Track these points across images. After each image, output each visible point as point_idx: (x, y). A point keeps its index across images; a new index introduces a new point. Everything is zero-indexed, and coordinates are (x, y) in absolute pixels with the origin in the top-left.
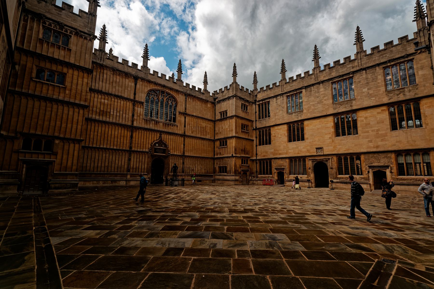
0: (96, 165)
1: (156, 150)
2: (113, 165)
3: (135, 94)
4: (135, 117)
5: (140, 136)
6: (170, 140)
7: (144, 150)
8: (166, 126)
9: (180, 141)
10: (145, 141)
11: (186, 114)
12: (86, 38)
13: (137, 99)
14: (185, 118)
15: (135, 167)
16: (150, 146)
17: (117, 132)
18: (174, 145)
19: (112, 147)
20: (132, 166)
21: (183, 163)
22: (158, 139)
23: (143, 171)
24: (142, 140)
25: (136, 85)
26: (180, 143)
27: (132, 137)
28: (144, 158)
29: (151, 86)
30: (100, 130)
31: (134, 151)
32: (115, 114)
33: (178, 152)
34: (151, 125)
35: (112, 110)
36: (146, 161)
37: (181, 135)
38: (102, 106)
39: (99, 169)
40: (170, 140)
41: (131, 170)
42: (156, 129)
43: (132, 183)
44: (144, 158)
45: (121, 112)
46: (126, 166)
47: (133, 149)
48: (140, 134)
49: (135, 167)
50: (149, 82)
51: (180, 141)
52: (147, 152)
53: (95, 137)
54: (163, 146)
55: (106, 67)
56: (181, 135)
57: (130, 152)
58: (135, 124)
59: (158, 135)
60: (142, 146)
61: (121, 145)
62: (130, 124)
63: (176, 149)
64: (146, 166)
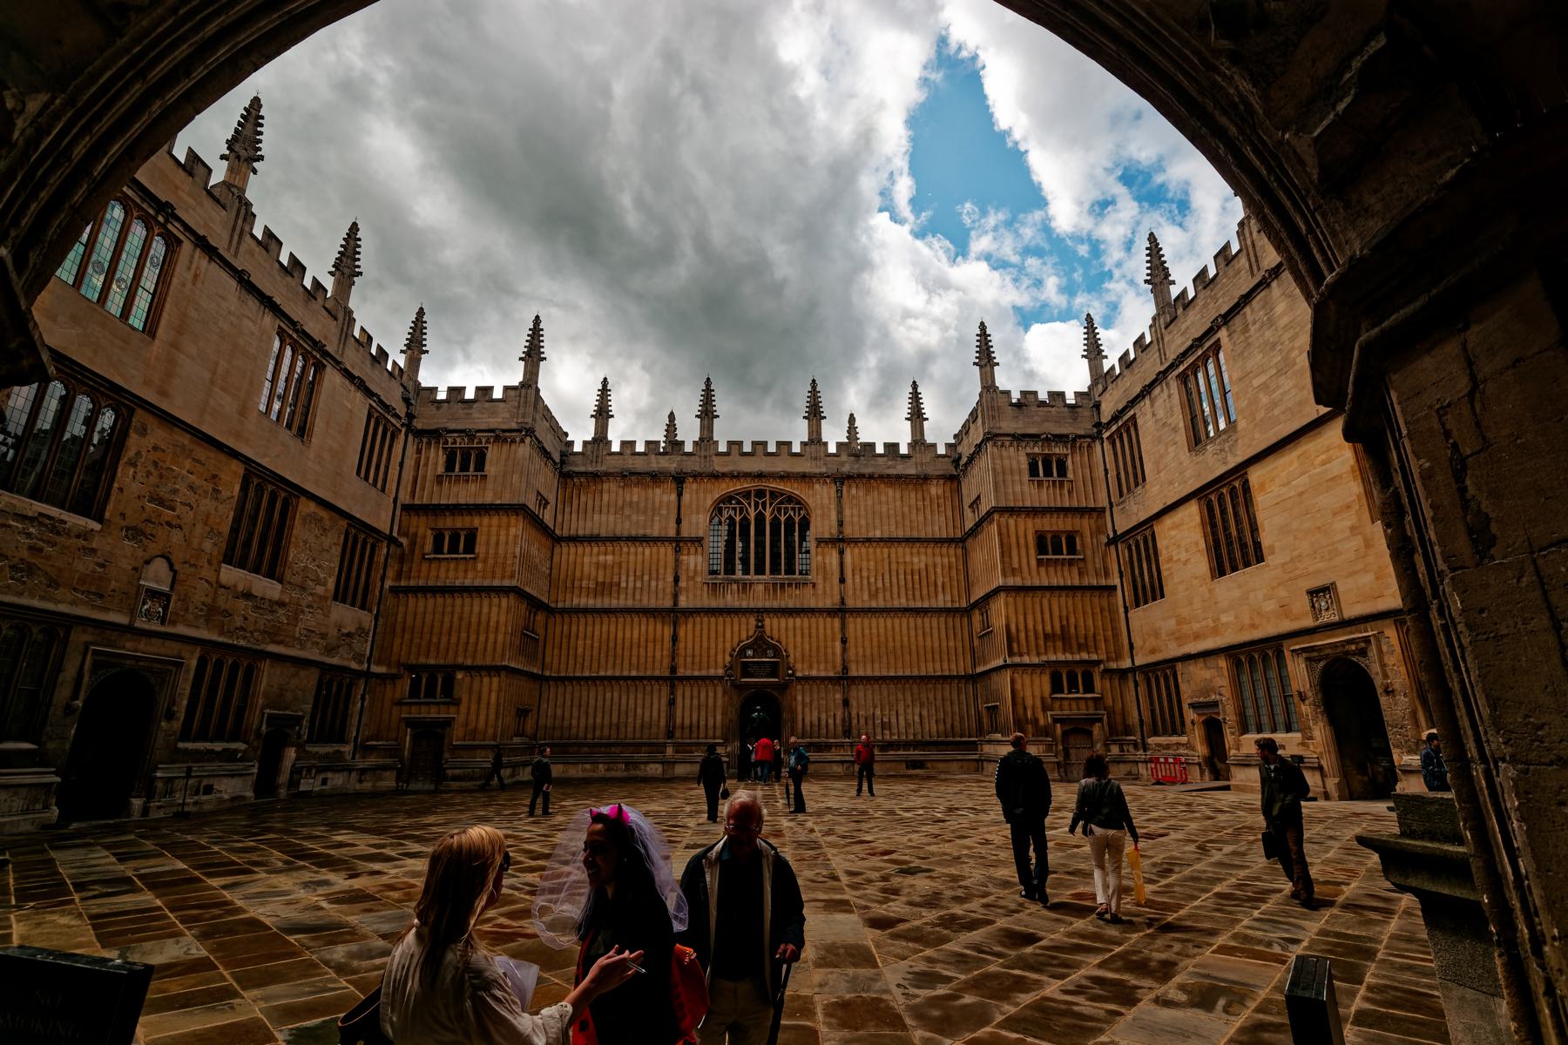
0: (591, 721)
1: (746, 669)
2: (630, 720)
3: (679, 521)
4: (682, 584)
5: (697, 633)
6: (791, 633)
7: (712, 672)
8: (775, 591)
10: (713, 645)
11: (842, 540)
12: (513, 441)
13: (685, 533)
14: (841, 553)
15: (687, 722)
16: (728, 659)
17: (636, 630)
18: (807, 647)
19: (626, 673)
20: (679, 721)
21: (846, 703)
23: (711, 733)
24: (705, 645)
25: (680, 495)
27: (675, 639)
28: (711, 694)
29: (724, 485)
30: (597, 633)
31: (681, 679)
32: (631, 585)
33: (822, 666)
34: (729, 597)
35: (624, 578)
36: (719, 702)
37: (831, 612)
38: (601, 573)
39: (598, 733)
40: (791, 633)
41: (678, 733)
42: (744, 605)
43: (680, 770)
44: (711, 694)
45: (646, 578)
46: (663, 722)
47: (681, 672)
48: (698, 627)
49: (687, 722)
50: (716, 476)
52: (720, 678)
53: (588, 653)
54: (770, 652)
55: (607, 474)
56: (831, 612)
57: (673, 680)
58: (683, 602)
59: (752, 621)
61: (649, 664)
62: (668, 603)
64: (719, 717)
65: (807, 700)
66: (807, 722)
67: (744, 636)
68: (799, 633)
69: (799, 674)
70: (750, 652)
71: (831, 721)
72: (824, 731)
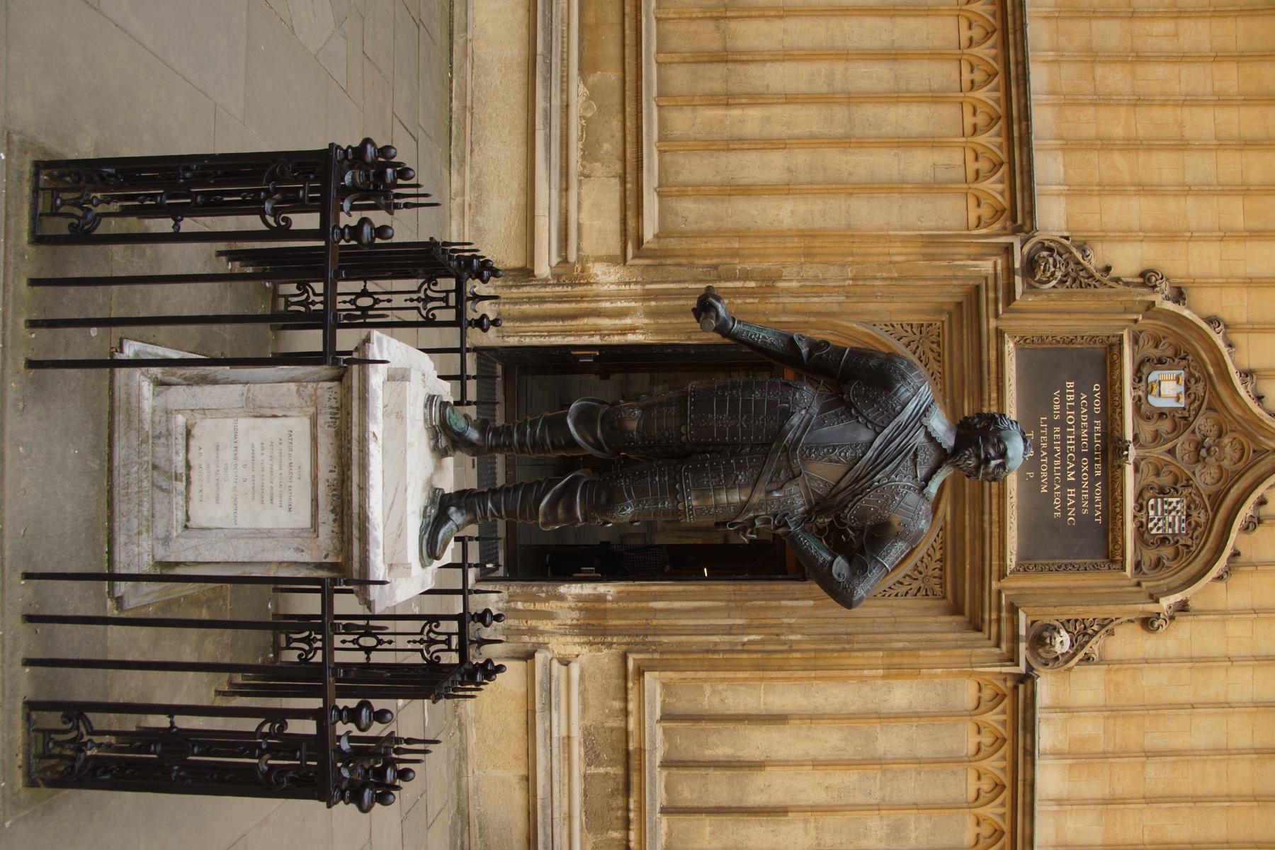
7: (1048, 167)
23: (696, 168)
28: (919, 163)
44: (919, 163)
52: (1019, 210)
54: (1169, 516)
60: (1116, 124)
63: (1124, 780)
64: (784, 213)
65: (890, 741)
66: (757, 742)
67: (1254, 351)
69: (1046, 688)
70: (1169, 389)
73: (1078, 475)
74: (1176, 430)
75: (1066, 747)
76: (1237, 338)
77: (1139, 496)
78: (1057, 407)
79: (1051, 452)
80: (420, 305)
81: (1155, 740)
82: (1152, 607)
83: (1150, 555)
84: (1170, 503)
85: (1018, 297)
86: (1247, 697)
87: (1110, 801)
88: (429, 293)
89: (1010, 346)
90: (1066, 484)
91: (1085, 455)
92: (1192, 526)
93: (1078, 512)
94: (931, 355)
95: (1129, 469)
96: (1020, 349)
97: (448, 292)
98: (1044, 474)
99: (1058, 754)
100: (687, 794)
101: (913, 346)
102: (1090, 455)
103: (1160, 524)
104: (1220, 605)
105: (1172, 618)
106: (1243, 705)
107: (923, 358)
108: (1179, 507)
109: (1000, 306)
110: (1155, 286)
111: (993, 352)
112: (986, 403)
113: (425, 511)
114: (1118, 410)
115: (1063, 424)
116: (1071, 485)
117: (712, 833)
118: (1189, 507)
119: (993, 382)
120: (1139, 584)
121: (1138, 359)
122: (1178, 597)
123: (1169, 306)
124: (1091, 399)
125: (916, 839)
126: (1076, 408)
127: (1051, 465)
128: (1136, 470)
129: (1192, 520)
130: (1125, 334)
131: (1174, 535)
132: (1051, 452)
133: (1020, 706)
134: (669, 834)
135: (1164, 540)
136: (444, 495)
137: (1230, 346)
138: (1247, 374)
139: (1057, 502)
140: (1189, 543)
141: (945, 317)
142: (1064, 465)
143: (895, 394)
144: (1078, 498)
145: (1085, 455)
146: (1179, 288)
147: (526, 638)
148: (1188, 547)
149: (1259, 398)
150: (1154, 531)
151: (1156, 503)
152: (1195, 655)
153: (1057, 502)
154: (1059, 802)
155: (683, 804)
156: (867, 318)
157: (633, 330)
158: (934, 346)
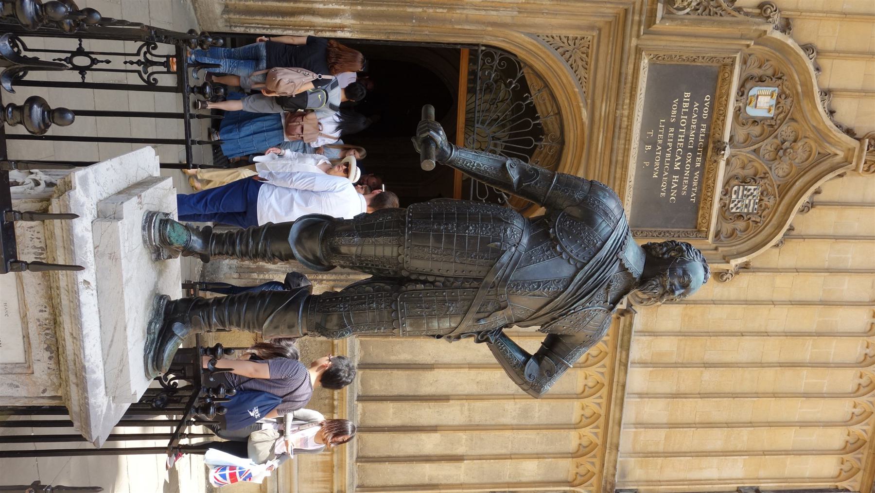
6: (813, 287)
9: (788, 438)
22: (848, 110)
26: (765, 438)
33: (656, 410)
40: (813, 287)
51: (788, 438)
54: (746, 200)
63: (687, 380)
68: (808, 319)
70: (763, 103)
71: (430, 443)
72: (390, 413)
73: (682, 166)
74: (762, 137)
75: (648, 359)
76: (824, 62)
77: (727, 183)
78: (674, 112)
79: (665, 147)
80: (141, 68)
81: (712, 356)
82: (724, 266)
83: (727, 227)
84: (750, 190)
85: (658, 22)
86: (780, 329)
87: (676, 396)
88: (148, 56)
89: (645, 62)
90: (672, 172)
91: (690, 150)
92: (762, 207)
93: (678, 195)
94: (580, 63)
95: (722, 164)
96: (652, 65)
97: (168, 57)
98: (657, 164)
99: (644, 364)
100: (377, 387)
101: (567, 55)
102: (694, 151)
103: (739, 205)
104: (773, 265)
105: (737, 273)
106: (777, 334)
107: (574, 65)
108: (755, 193)
109: (642, 28)
110: (769, 17)
111: (631, 66)
112: (620, 107)
113: (149, 329)
114: (722, 118)
115: (677, 126)
116: (676, 173)
117: (394, 413)
118: (762, 194)
119: (628, 91)
120: (716, 249)
121: (743, 77)
122: (744, 259)
123: (778, 35)
124: (701, 108)
125: (539, 417)
126: (689, 114)
127: (663, 157)
128: (728, 163)
129: (763, 203)
130: (738, 56)
131: (748, 214)
132: (665, 147)
133: (620, 332)
134: (364, 414)
135: (740, 216)
136: (170, 303)
137: (818, 69)
138: (826, 93)
139: (664, 186)
140: (758, 220)
141: (595, 33)
142: (673, 157)
143: (597, 230)
144: (680, 183)
145: (690, 150)
146: (787, 19)
147: (255, 275)
148: (757, 222)
149: (832, 113)
150: (734, 210)
151: (739, 189)
152: (749, 298)
153: (664, 186)
154: (641, 395)
155: (374, 394)
156: (533, 30)
157: (342, 28)
158: (584, 56)
